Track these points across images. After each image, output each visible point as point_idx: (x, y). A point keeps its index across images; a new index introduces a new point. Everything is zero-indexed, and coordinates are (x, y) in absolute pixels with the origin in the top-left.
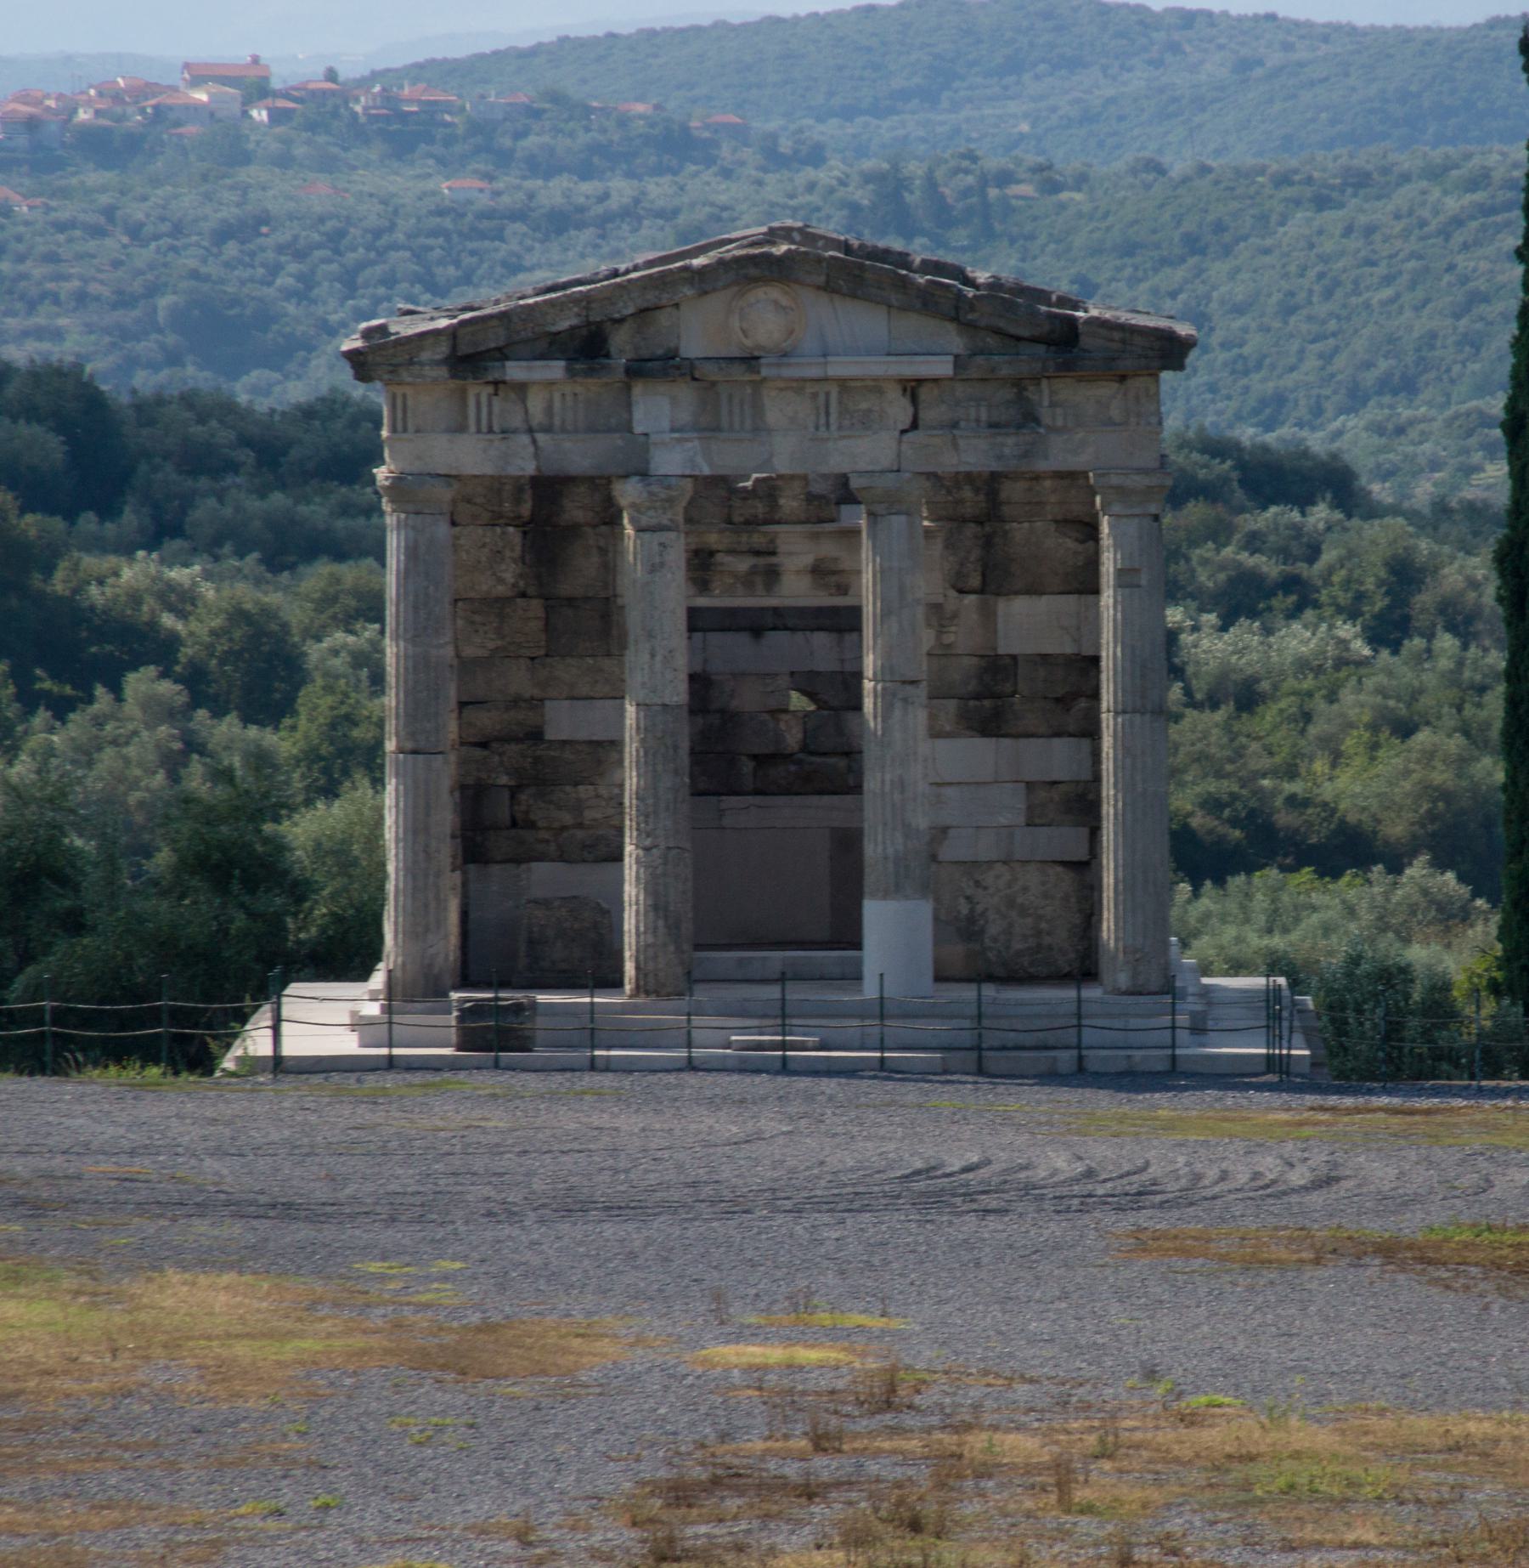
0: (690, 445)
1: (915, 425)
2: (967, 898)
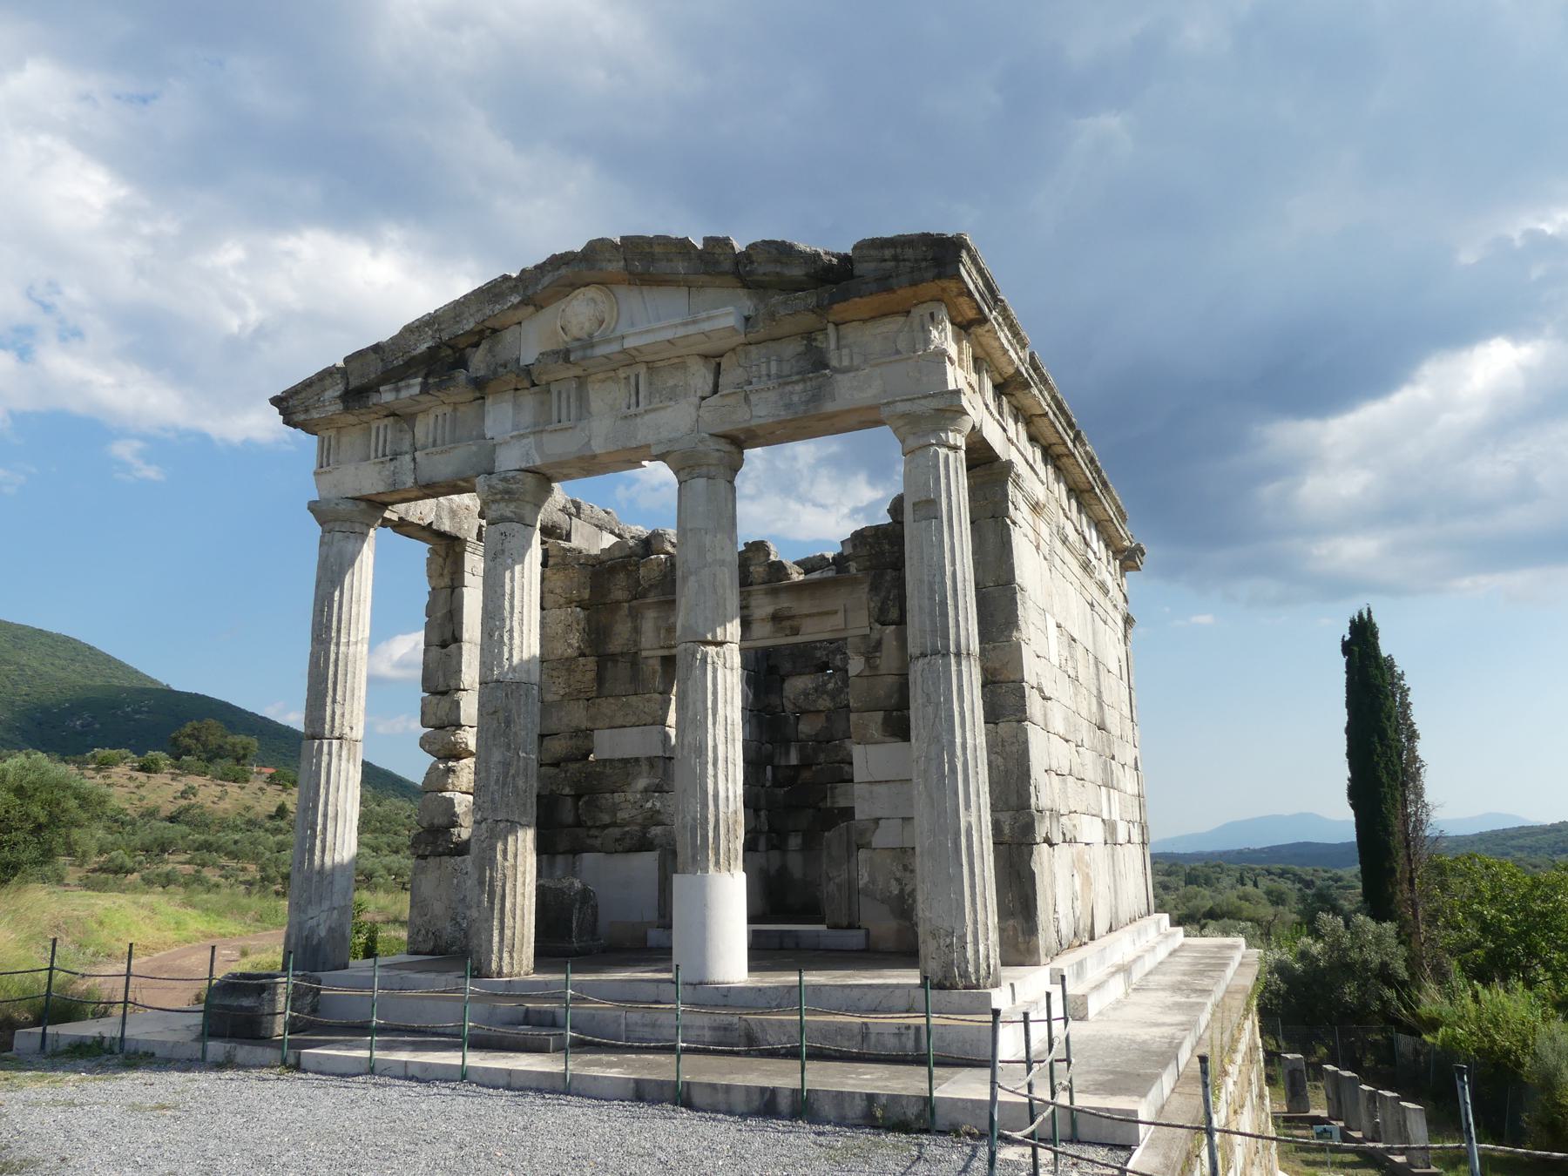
0: (525, 441)
1: (715, 391)
2: (897, 880)
